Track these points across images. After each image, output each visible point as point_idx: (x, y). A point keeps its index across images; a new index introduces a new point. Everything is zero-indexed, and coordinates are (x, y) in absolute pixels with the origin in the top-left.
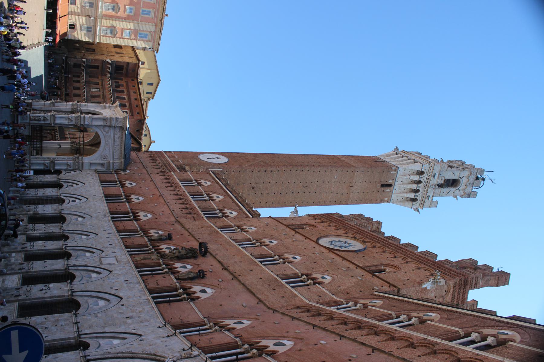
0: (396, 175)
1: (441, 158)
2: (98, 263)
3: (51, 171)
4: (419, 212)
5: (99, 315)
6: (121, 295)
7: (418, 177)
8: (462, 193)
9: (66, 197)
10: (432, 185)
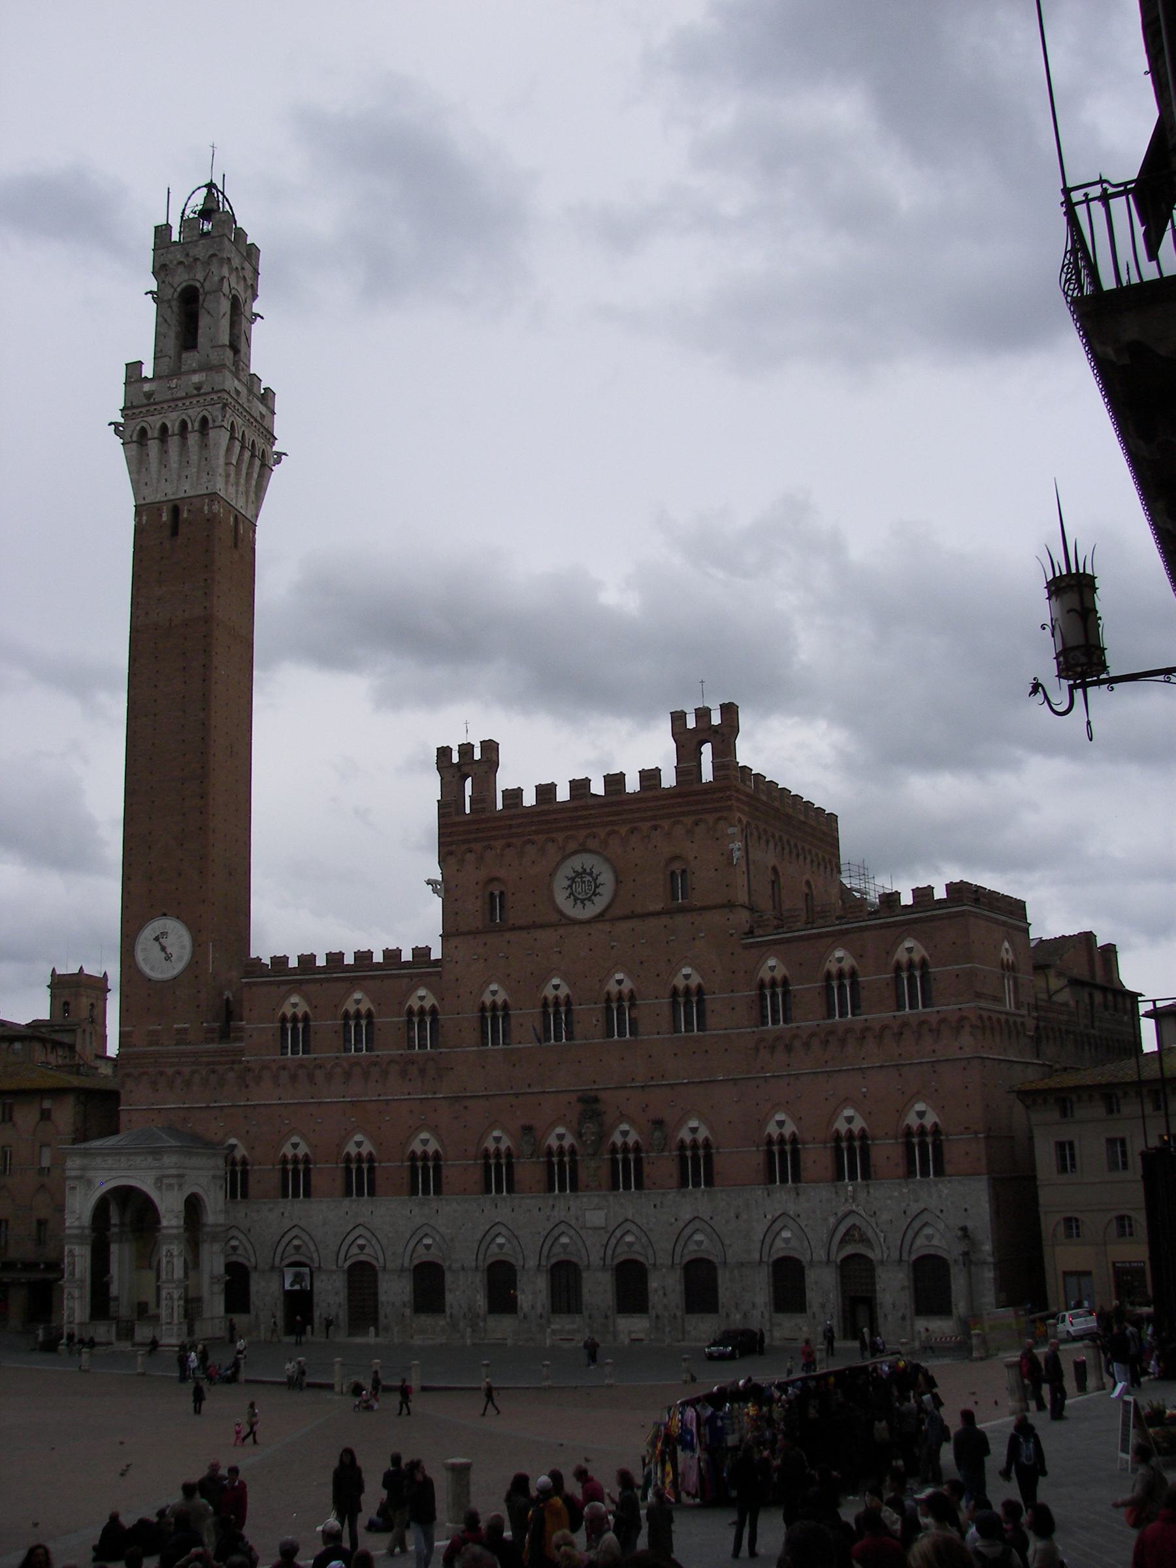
0: (225, 503)
1: (146, 294)
4: (285, 454)
5: (727, 1242)
6: (688, 1217)
7: (237, 442)
8: (250, 292)
9: (345, 1260)
10: (248, 400)
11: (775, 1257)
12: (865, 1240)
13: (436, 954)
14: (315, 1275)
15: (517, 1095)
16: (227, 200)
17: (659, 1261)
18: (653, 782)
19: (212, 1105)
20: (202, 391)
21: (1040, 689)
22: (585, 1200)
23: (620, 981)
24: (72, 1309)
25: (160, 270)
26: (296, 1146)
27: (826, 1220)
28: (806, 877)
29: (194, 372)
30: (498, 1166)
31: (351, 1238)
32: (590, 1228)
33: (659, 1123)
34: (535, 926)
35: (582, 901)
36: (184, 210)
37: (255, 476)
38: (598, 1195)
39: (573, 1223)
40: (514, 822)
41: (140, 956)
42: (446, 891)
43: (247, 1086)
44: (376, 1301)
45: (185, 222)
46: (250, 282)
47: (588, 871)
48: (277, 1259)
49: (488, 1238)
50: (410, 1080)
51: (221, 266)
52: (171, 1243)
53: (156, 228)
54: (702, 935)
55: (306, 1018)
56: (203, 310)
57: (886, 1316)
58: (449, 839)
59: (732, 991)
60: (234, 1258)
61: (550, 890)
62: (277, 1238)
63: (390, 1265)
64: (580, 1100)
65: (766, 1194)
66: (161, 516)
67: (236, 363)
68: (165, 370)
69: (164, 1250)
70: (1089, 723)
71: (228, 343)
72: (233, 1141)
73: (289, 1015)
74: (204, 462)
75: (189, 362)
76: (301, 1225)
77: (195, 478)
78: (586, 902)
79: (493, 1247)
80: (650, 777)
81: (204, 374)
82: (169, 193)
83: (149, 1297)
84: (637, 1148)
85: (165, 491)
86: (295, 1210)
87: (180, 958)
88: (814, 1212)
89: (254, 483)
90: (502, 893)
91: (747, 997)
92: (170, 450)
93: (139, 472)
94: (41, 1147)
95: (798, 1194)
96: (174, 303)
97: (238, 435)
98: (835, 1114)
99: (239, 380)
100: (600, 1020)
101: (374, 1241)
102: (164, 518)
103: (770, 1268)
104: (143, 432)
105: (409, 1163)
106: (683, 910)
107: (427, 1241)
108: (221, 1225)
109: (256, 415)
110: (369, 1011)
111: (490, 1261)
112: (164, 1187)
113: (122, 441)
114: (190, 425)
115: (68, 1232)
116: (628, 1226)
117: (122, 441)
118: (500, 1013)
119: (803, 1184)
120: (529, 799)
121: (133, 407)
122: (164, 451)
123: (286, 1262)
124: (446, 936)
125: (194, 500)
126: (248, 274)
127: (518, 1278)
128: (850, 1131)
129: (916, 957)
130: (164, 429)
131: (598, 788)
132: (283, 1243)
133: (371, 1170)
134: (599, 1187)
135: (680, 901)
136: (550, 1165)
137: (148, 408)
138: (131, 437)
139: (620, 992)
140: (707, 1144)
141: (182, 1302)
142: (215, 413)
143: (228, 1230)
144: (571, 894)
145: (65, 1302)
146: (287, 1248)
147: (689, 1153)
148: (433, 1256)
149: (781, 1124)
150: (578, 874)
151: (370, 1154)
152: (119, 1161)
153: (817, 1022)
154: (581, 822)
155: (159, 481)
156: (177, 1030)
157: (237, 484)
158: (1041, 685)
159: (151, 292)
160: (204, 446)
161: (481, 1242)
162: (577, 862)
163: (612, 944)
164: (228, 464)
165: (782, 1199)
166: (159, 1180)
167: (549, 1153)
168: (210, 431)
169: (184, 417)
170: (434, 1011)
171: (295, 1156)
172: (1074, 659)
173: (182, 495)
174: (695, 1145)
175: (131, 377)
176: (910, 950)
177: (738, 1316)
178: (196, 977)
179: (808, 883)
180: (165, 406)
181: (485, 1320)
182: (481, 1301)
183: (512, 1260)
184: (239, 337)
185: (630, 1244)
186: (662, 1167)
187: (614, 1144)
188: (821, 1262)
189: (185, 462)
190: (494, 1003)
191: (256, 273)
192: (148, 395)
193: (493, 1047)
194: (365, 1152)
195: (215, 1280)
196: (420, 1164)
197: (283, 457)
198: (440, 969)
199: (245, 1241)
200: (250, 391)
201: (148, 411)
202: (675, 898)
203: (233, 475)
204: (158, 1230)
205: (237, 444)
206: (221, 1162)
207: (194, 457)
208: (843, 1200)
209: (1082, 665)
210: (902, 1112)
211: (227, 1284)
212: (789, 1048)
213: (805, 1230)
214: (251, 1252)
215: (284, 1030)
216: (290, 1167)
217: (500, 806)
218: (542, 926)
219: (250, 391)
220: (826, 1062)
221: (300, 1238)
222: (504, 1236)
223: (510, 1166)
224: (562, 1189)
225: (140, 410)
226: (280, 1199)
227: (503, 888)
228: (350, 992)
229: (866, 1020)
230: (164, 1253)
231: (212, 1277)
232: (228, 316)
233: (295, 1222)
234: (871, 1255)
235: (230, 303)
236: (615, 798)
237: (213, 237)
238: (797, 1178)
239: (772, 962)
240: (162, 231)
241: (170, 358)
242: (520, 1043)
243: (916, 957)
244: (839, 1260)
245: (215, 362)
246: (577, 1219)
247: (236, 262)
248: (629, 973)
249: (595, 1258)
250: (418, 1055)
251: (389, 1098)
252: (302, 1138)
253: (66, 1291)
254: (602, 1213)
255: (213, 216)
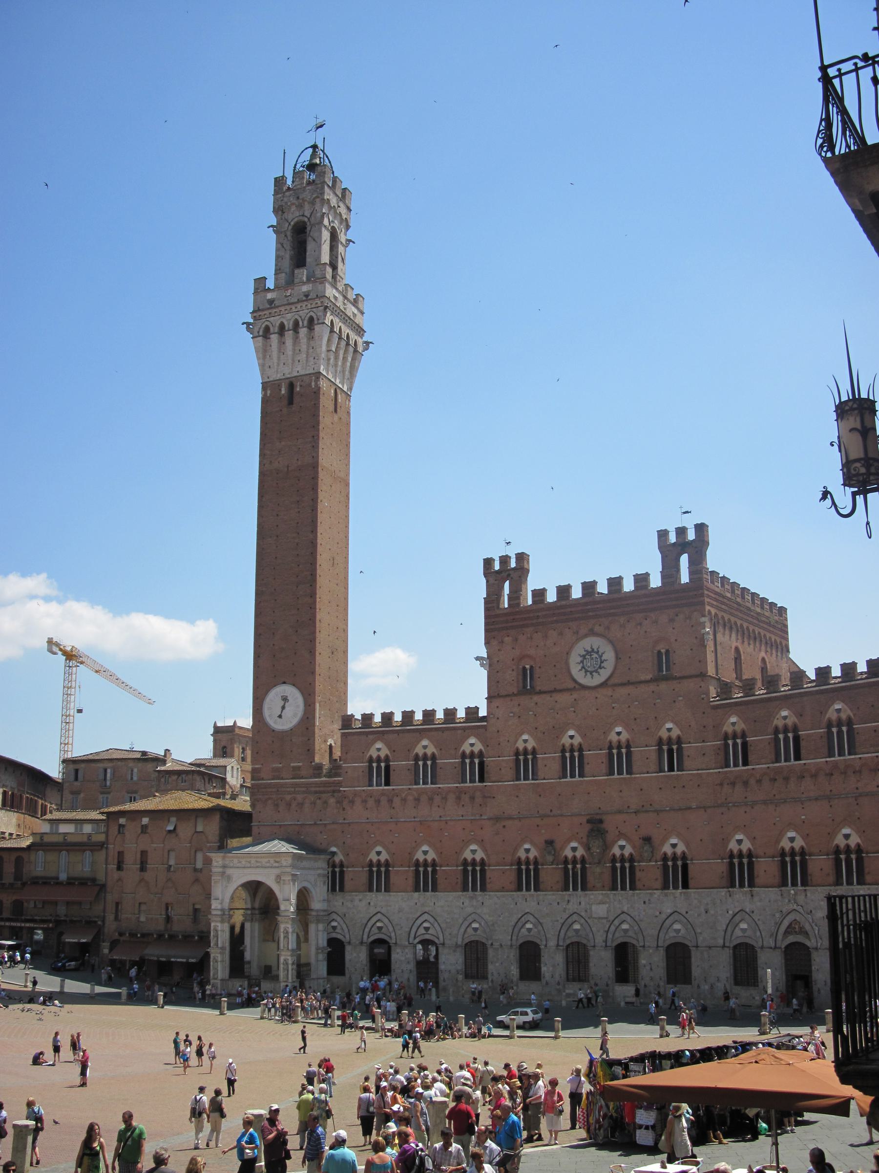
1: (269, 227)
2: (604, 921)
3: (329, 952)
4: (371, 343)
5: (699, 931)
6: (669, 911)
7: (335, 335)
9: (415, 938)
10: (344, 304)
11: (735, 943)
12: (804, 932)
13: (483, 713)
14: (393, 948)
15: (543, 817)
16: (327, 157)
17: (647, 944)
18: (644, 583)
19: (318, 823)
20: (309, 297)
21: (829, 496)
22: (592, 897)
23: (619, 733)
24: (216, 969)
25: (279, 210)
26: (379, 854)
27: (774, 915)
28: (763, 654)
29: (304, 283)
30: (528, 871)
31: (419, 922)
32: (595, 918)
33: (647, 840)
34: (555, 691)
35: (591, 673)
36: (296, 165)
37: (350, 359)
38: (602, 894)
39: (583, 914)
40: (540, 614)
41: (266, 713)
42: (490, 665)
43: (344, 809)
44: (437, 969)
45: (296, 174)
46: (344, 217)
47: (596, 650)
48: (365, 937)
49: (520, 924)
50: (463, 805)
51: (323, 206)
52: (287, 923)
53: (276, 179)
54: (681, 698)
55: (387, 760)
56: (310, 238)
57: (819, 990)
58: (492, 627)
59: (703, 741)
60: (334, 935)
61: (567, 664)
62: (365, 921)
63: (447, 942)
64: (588, 821)
65: (728, 894)
66: (280, 390)
67: (334, 277)
68: (282, 282)
69: (282, 927)
70: (868, 523)
71: (328, 262)
72: (334, 849)
73: (375, 756)
74: (311, 350)
75: (300, 276)
76: (383, 911)
77: (305, 362)
78: (594, 674)
79: (523, 930)
80: (641, 580)
81: (311, 285)
82: (284, 153)
83: (272, 962)
84: (631, 859)
85: (284, 371)
86: (378, 900)
87: (295, 715)
88: (764, 910)
89: (348, 364)
90: (531, 667)
91: (714, 745)
92: (287, 341)
93: (264, 358)
94: (196, 852)
95: (752, 896)
96: (289, 234)
97: (336, 329)
98: (781, 834)
99: (337, 289)
100: (604, 761)
101: (436, 925)
102: (283, 392)
103: (731, 951)
104: (267, 330)
105: (462, 868)
106: (666, 678)
107: (475, 925)
108: (325, 911)
109: (350, 314)
110: (433, 755)
111: (521, 941)
112: (282, 882)
113: (252, 336)
114: (301, 323)
115: (214, 912)
116: (623, 916)
117: (252, 336)
118: (530, 757)
119: (756, 889)
120: (551, 597)
121: (259, 310)
122: (282, 343)
123: (372, 939)
124: (490, 699)
125: (305, 378)
126: (343, 210)
127: (542, 954)
128: (792, 848)
129: (844, 716)
130: (282, 328)
131: (603, 588)
132: (370, 925)
133: (434, 872)
134: (603, 888)
135: (664, 673)
136: (566, 870)
137: (270, 311)
138: (258, 332)
139: (619, 742)
140: (684, 857)
141: (295, 967)
142: (320, 314)
143: (329, 914)
144: (583, 667)
145: (211, 963)
146: (373, 929)
147: (670, 863)
148: (480, 936)
149: (740, 842)
150: (588, 652)
151: (434, 860)
152: (250, 862)
153: (768, 765)
154: (591, 614)
155: (278, 365)
156: (293, 767)
157: (336, 365)
158: (829, 493)
159: (272, 226)
160: (311, 338)
161: (515, 927)
162: (587, 643)
163: (613, 705)
164: (328, 351)
165: (740, 897)
166: (278, 879)
167: (566, 861)
168: (316, 327)
169: (297, 317)
170: (481, 754)
171: (379, 861)
172: (855, 470)
173: (296, 374)
174: (675, 858)
175: (258, 289)
176: (838, 711)
177: (707, 987)
178: (307, 729)
179: (763, 659)
180: (282, 309)
181: (517, 986)
182: (515, 971)
183: (538, 941)
184: (337, 257)
185: (626, 931)
186: (649, 871)
187: (614, 855)
188: (771, 948)
189: (296, 351)
190: (525, 749)
191: (349, 209)
192: (271, 302)
193: (524, 782)
194: (429, 859)
195: (320, 951)
196: (470, 868)
197: (370, 345)
198: (485, 723)
199: (342, 922)
200: (345, 297)
201: (270, 313)
202: (660, 669)
203: (332, 358)
204: (278, 914)
205: (335, 338)
206: (325, 865)
207: (304, 347)
208: (787, 901)
209: (863, 474)
210: (832, 835)
211: (329, 955)
212: (746, 783)
213: (757, 922)
214: (346, 930)
215: (370, 768)
216: (375, 869)
217: (530, 602)
218: (561, 691)
219: (345, 297)
220: (774, 795)
221: (382, 922)
222: (531, 923)
223: (536, 870)
224: (575, 889)
225: (264, 313)
226: (368, 893)
227: (532, 663)
228: (421, 740)
229: (805, 764)
230: (282, 930)
231: (317, 949)
232: (328, 242)
233: (378, 909)
234: (808, 943)
235: (329, 235)
236: (616, 596)
237: (317, 184)
238: (752, 885)
239: (733, 719)
240: (279, 182)
241: (286, 273)
242: (544, 779)
243: (844, 716)
244: (783, 947)
245: (319, 276)
246: (586, 911)
247: (334, 202)
248: (627, 727)
249: (600, 940)
250: (469, 787)
251: (448, 818)
252: (384, 847)
253: (212, 956)
254: (605, 906)
255: (316, 168)
